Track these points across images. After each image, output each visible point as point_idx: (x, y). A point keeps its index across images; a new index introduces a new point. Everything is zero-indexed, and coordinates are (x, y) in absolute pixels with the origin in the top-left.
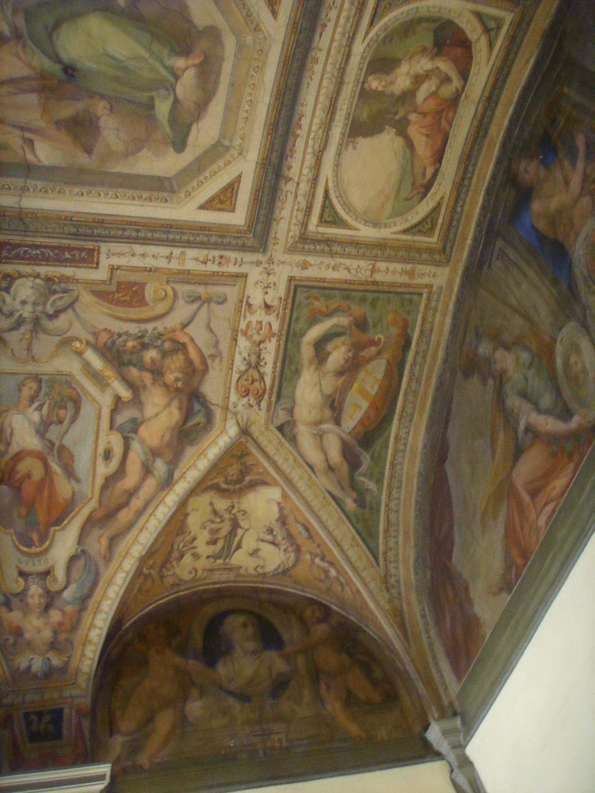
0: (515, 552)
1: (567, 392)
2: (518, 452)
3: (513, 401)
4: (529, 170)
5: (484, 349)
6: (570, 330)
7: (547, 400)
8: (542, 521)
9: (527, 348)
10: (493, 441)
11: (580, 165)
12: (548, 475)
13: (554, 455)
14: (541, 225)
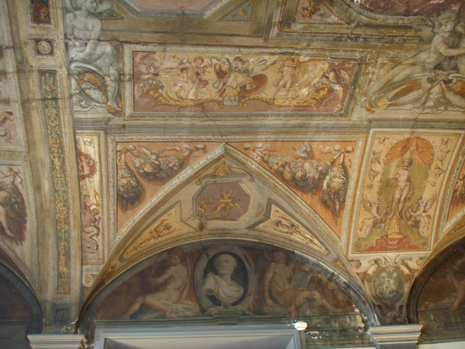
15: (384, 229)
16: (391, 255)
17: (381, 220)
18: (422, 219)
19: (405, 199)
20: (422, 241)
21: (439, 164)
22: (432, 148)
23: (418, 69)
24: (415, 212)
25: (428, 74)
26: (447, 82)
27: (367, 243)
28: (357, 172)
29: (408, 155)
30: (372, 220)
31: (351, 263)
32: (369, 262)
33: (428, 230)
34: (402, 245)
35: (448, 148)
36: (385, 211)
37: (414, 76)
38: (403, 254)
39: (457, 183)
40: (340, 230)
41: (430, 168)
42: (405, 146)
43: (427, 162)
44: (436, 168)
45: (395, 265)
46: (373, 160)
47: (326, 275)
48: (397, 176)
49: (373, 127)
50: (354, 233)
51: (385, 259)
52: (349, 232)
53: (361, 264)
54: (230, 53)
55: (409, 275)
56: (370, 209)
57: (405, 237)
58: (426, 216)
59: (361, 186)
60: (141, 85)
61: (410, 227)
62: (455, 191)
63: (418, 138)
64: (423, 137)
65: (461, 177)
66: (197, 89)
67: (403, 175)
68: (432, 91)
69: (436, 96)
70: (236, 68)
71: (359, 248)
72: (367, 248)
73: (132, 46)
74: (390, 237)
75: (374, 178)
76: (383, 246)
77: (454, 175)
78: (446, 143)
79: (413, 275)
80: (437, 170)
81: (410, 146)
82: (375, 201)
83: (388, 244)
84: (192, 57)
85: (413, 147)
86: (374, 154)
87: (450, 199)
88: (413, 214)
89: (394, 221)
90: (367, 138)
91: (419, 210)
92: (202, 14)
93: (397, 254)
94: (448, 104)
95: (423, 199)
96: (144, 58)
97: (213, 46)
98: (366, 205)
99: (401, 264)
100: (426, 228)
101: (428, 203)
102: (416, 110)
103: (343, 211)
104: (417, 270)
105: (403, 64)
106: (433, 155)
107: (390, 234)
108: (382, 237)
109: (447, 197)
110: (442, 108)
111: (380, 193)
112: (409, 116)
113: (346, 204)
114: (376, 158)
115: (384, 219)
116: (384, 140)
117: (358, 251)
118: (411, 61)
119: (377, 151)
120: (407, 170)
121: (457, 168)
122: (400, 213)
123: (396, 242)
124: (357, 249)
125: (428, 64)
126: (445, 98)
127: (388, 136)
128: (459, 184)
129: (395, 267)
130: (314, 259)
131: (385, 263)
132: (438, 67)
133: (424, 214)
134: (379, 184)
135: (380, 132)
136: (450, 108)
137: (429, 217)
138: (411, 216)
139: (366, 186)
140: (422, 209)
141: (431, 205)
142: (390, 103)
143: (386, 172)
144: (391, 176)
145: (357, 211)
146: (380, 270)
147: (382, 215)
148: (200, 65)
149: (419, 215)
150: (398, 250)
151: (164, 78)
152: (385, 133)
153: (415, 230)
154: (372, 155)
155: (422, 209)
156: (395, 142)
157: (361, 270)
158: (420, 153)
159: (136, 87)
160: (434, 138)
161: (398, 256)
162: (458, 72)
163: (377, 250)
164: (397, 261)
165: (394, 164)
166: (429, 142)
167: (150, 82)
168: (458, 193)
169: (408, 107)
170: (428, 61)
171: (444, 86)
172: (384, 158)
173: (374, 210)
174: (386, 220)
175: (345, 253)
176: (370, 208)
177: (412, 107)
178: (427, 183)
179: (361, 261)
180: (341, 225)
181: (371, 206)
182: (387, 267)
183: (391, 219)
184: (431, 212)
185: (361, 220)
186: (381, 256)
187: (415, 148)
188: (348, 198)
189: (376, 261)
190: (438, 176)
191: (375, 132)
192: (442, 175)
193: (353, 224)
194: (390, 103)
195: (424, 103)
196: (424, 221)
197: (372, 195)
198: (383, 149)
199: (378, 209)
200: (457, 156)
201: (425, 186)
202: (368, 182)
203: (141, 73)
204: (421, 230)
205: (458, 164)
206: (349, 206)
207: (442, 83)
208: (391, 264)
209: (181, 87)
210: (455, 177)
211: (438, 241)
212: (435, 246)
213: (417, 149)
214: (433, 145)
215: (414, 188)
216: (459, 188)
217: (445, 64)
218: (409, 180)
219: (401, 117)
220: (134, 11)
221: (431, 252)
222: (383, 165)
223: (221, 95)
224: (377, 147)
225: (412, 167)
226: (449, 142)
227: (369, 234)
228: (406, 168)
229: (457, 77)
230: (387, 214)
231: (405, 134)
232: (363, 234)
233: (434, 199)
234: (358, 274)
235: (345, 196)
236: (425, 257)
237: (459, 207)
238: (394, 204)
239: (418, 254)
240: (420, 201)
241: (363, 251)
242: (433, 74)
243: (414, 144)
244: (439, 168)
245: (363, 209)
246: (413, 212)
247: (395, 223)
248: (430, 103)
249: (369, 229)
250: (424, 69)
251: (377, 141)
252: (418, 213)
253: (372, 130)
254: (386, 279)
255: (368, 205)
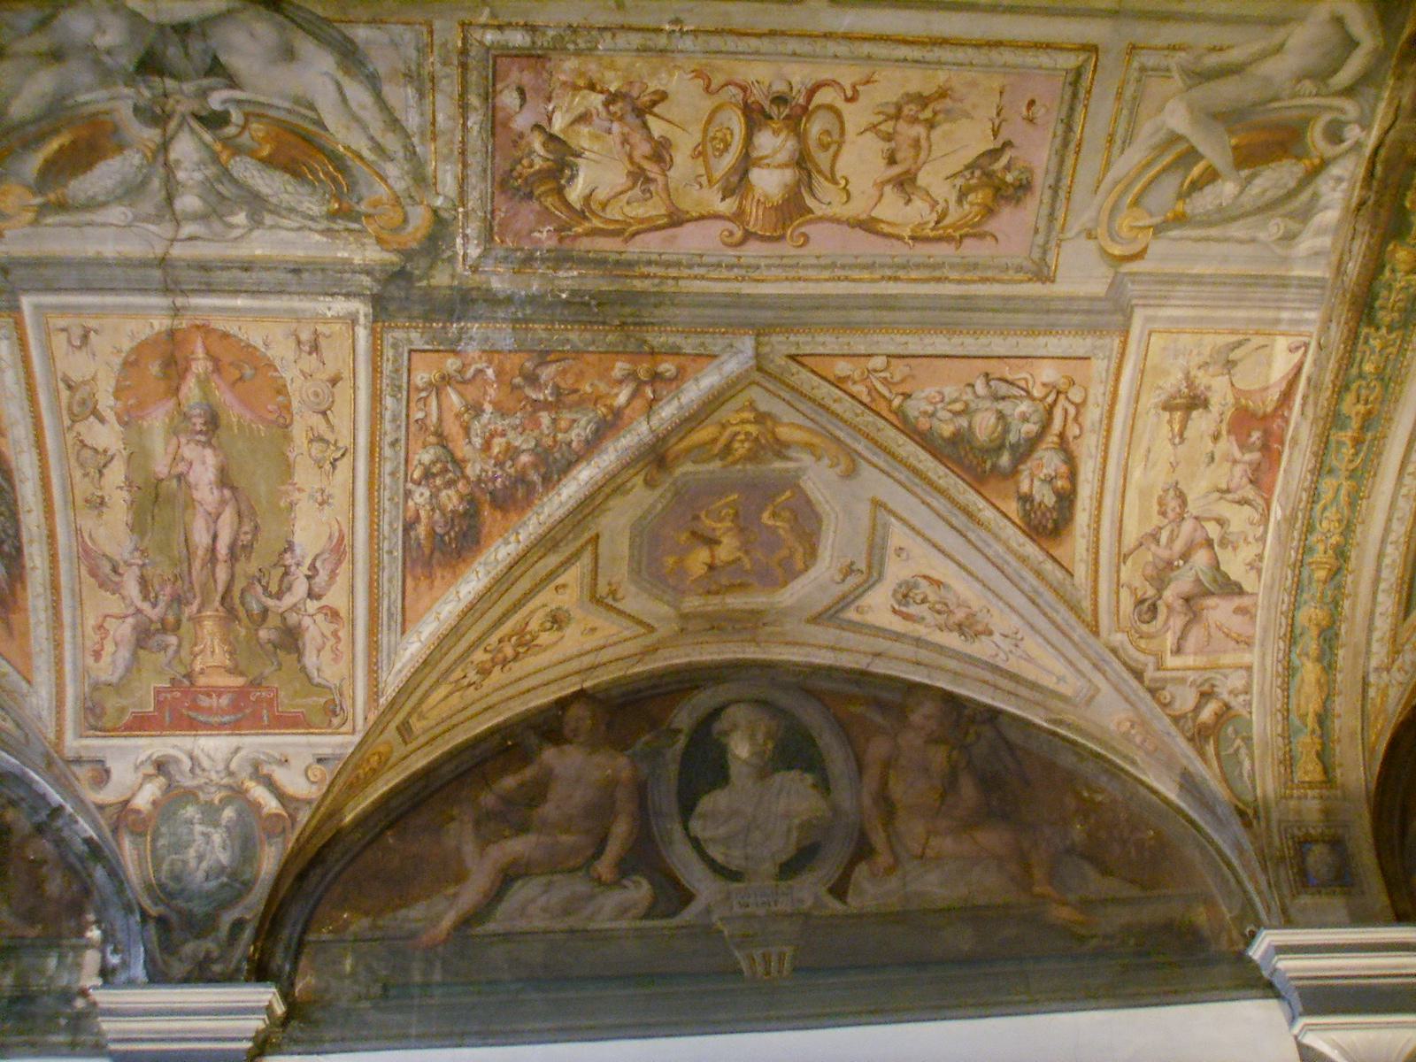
15: (177, 651)
16: (213, 749)
17: (163, 621)
18: (307, 621)
19: (232, 548)
20: (322, 701)
21: (317, 421)
22: (271, 366)
23: (79, 72)
24: (279, 596)
25: (126, 91)
26: (214, 121)
27: (124, 702)
28: (34, 452)
29: (191, 390)
30: (130, 620)
31: (75, 768)
32: (137, 768)
33: (336, 659)
34: (248, 711)
35: (331, 371)
36: (168, 590)
37: (82, 98)
38: (254, 744)
39: (408, 494)
40: (27, 656)
41: (287, 438)
42: (170, 355)
43: (272, 417)
44: (311, 441)
45: (226, 781)
46: (76, 409)
47: (34, 810)
48: (182, 467)
49: (26, 291)
50: (75, 664)
51: (192, 758)
52: (59, 662)
53: (107, 772)
55: (278, 816)
56: (117, 583)
57: (255, 684)
58: (320, 609)
59: (66, 502)
61: (269, 647)
62: (408, 528)
63: (205, 329)
64: (219, 324)
65: (416, 475)
67: (203, 468)
68: (172, 156)
69: (198, 176)
71: (99, 717)
72: (127, 718)
74: (202, 681)
75: (101, 473)
76: (180, 710)
77: (388, 467)
78: (315, 348)
79: (293, 818)
80: (315, 445)
81: (188, 361)
82: (126, 556)
83: (195, 707)
85: (200, 366)
86: (70, 387)
87: (398, 553)
88: (271, 603)
89: (209, 625)
90: (19, 325)
91: (289, 589)
93: (235, 741)
94: (257, 204)
95: (298, 551)
98: (105, 574)
99: (251, 778)
100: (327, 655)
101: (318, 564)
102: (152, 227)
103: (24, 588)
104: (309, 802)
105: (16, 55)
106: (281, 390)
107: (202, 672)
108: (173, 680)
109: (386, 546)
110: (240, 218)
111: (138, 526)
112: (134, 248)
113: (28, 564)
114: (83, 403)
115: (171, 618)
116: (85, 337)
117: (96, 729)
118: (42, 42)
119: (76, 377)
120: (208, 444)
121: (388, 439)
122: (223, 598)
123: (224, 701)
124: (92, 720)
125: (109, 52)
126: (234, 181)
127: (92, 323)
128: (417, 496)
129: (229, 787)
130: (13, 760)
131: (192, 770)
132: (150, 65)
133: (312, 606)
134: (125, 494)
135: (63, 310)
136: (269, 219)
137: (334, 614)
138: (265, 611)
139: (79, 502)
140: (300, 588)
141: (333, 575)
142: (39, 200)
143: (137, 456)
144: (161, 467)
145: (73, 590)
146: (175, 796)
147: (162, 605)
149: (294, 608)
150: (235, 727)
152: (78, 310)
153: (289, 659)
154: (65, 394)
155: (300, 588)
156: (127, 345)
157: (108, 795)
158: (234, 384)
160: (261, 324)
161: (238, 749)
162: (232, 82)
163: (163, 728)
164: (233, 766)
165: (157, 420)
166: (249, 345)
168: (421, 530)
169: (116, 214)
170: (104, 41)
171: (208, 137)
172: (111, 402)
173: (132, 589)
174: (178, 623)
175: (52, 736)
176: (116, 579)
177: (130, 216)
178: (297, 495)
179: (109, 764)
180: (25, 634)
181: (115, 570)
182: (200, 787)
183: (197, 620)
184: (335, 597)
185: (91, 622)
186: (174, 746)
187: (210, 365)
188: (31, 541)
189: (161, 766)
190: (328, 467)
191: (38, 307)
192: (343, 465)
193: (67, 634)
194: (39, 200)
195: (170, 199)
196: (314, 629)
197: (112, 532)
198: (98, 369)
199: (144, 582)
200: (376, 398)
201: (292, 505)
202: (83, 487)
204: (310, 660)
205: (388, 426)
206: (39, 572)
207: (196, 125)
208: (214, 776)
210: (393, 474)
211: (382, 701)
212: (372, 718)
213: (217, 368)
214: (269, 354)
215: (254, 514)
216: (423, 514)
217: (173, 52)
218: (224, 479)
219: (110, 250)
221: (357, 739)
222: (117, 427)
224: (77, 366)
225: (222, 433)
226: (323, 342)
227: (128, 669)
228: (203, 438)
229: (239, 103)
230: (178, 600)
231: (147, 317)
232: (109, 667)
233: (339, 549)
234: (101, 807)
235: (17, 536)
236: (337, 758)
237: (437, 583)
238: (197, 564)
239: (310, 745)
240: (288, 559)
241: (114, 730)
242: (147, 94)
243: (200, 353)
244: (321, 439)
245: (92, 580)
246: (270, 596)
247: (213, 634)
248: (188, 202)
249: (124, 654)
250: (106, 76)
251: (60, 341)
252: (288, 600)
253: (27, 302)
254: (198, 828)
255: (106, 568)
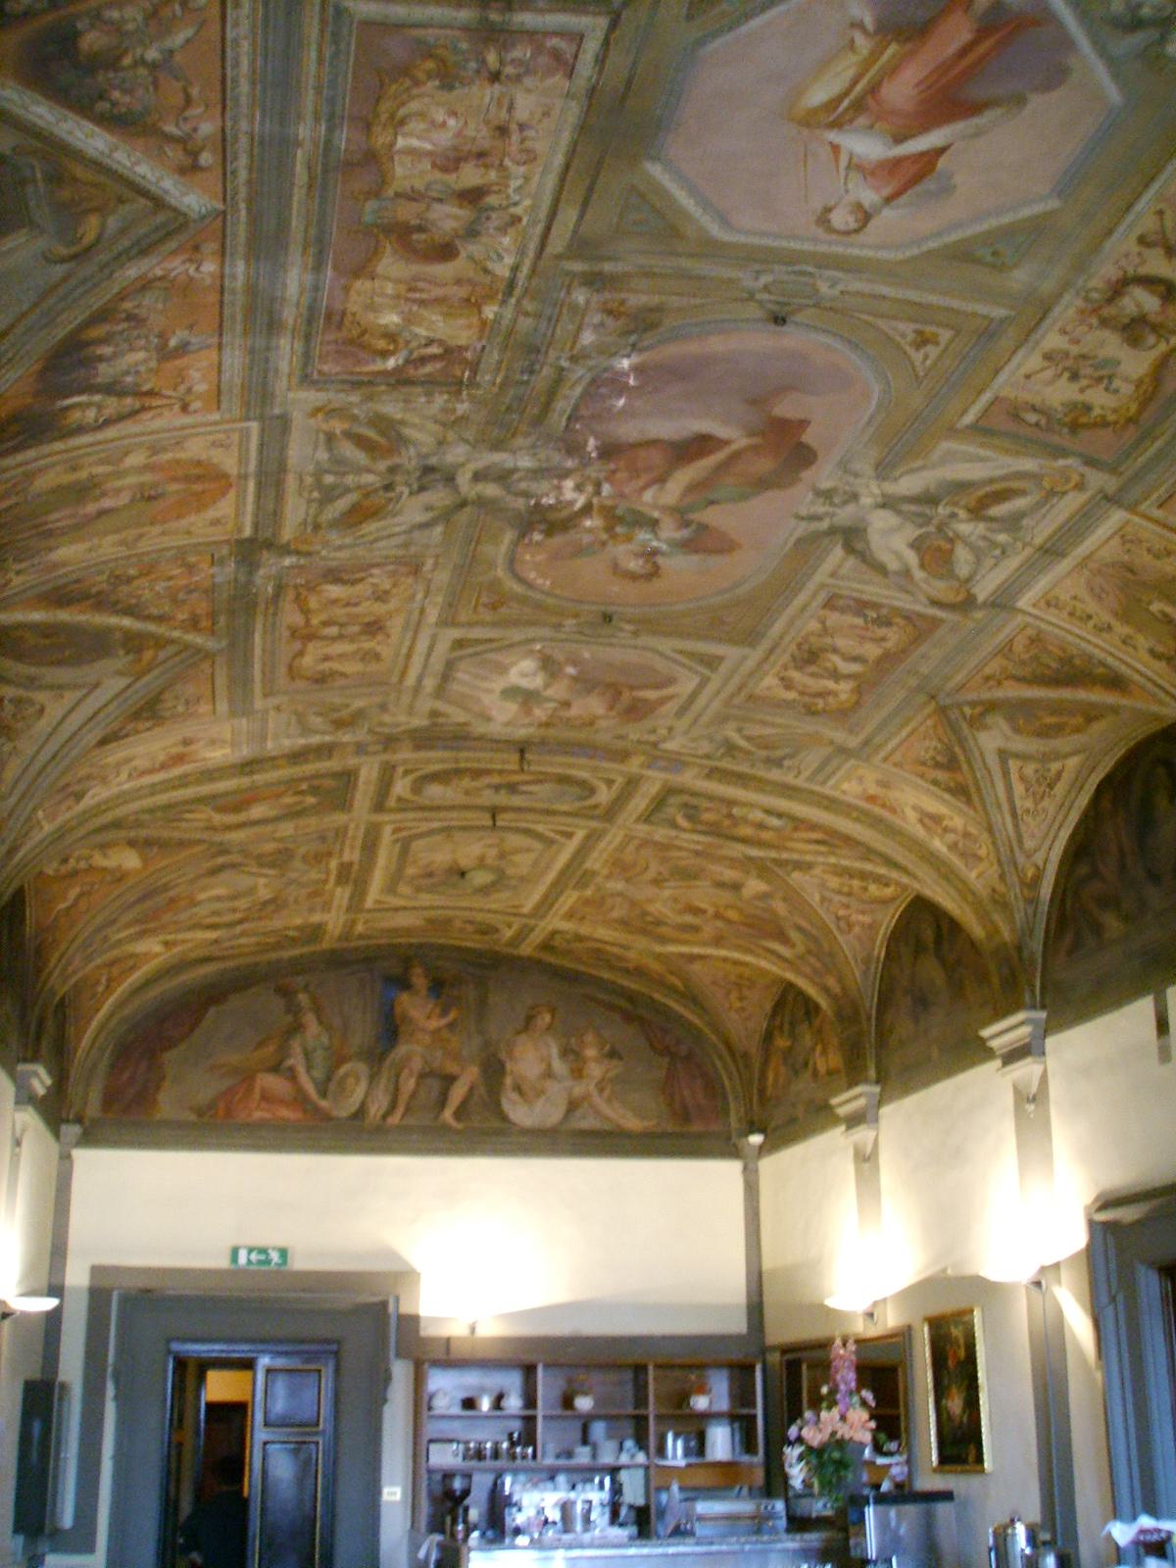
0: (221, 1105)
1: (332, 1087)
2: (275, 1069)
3: (296, 1046)
4: (419, 979)
5: (303, 998)
6: (362, 1068)
7: (319, 1074)
8: (258, 1115)
9: (330, 1038)
10: (261, 1044)
11: (443, 1022)
12: (282, 1102)
13: (295, 1099)
14: (398, 1010)
54: (534, 208)
60: (464, 46)
66: (429, 154)
70: (488, 218)
73: (600, 35)
84: (540, 146)
92: (655, 159)
96: (556, 55)
97: (563, 179)
148: (512, 160)
151: (484, 94)
159: (457, 33)
167: (473, 65)
203: (505, 47)
209: (444, 124)
220: (701, 42)
223: (397, 195)
